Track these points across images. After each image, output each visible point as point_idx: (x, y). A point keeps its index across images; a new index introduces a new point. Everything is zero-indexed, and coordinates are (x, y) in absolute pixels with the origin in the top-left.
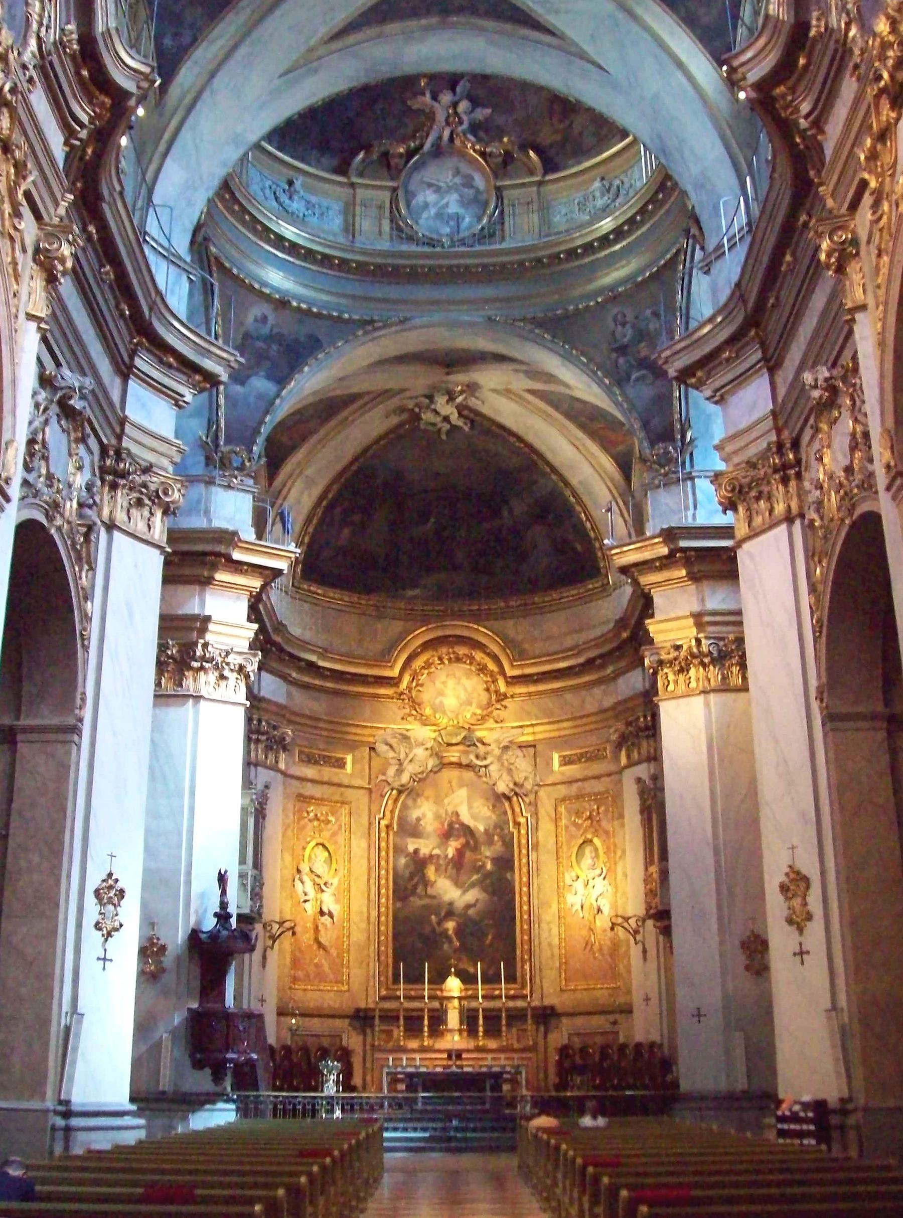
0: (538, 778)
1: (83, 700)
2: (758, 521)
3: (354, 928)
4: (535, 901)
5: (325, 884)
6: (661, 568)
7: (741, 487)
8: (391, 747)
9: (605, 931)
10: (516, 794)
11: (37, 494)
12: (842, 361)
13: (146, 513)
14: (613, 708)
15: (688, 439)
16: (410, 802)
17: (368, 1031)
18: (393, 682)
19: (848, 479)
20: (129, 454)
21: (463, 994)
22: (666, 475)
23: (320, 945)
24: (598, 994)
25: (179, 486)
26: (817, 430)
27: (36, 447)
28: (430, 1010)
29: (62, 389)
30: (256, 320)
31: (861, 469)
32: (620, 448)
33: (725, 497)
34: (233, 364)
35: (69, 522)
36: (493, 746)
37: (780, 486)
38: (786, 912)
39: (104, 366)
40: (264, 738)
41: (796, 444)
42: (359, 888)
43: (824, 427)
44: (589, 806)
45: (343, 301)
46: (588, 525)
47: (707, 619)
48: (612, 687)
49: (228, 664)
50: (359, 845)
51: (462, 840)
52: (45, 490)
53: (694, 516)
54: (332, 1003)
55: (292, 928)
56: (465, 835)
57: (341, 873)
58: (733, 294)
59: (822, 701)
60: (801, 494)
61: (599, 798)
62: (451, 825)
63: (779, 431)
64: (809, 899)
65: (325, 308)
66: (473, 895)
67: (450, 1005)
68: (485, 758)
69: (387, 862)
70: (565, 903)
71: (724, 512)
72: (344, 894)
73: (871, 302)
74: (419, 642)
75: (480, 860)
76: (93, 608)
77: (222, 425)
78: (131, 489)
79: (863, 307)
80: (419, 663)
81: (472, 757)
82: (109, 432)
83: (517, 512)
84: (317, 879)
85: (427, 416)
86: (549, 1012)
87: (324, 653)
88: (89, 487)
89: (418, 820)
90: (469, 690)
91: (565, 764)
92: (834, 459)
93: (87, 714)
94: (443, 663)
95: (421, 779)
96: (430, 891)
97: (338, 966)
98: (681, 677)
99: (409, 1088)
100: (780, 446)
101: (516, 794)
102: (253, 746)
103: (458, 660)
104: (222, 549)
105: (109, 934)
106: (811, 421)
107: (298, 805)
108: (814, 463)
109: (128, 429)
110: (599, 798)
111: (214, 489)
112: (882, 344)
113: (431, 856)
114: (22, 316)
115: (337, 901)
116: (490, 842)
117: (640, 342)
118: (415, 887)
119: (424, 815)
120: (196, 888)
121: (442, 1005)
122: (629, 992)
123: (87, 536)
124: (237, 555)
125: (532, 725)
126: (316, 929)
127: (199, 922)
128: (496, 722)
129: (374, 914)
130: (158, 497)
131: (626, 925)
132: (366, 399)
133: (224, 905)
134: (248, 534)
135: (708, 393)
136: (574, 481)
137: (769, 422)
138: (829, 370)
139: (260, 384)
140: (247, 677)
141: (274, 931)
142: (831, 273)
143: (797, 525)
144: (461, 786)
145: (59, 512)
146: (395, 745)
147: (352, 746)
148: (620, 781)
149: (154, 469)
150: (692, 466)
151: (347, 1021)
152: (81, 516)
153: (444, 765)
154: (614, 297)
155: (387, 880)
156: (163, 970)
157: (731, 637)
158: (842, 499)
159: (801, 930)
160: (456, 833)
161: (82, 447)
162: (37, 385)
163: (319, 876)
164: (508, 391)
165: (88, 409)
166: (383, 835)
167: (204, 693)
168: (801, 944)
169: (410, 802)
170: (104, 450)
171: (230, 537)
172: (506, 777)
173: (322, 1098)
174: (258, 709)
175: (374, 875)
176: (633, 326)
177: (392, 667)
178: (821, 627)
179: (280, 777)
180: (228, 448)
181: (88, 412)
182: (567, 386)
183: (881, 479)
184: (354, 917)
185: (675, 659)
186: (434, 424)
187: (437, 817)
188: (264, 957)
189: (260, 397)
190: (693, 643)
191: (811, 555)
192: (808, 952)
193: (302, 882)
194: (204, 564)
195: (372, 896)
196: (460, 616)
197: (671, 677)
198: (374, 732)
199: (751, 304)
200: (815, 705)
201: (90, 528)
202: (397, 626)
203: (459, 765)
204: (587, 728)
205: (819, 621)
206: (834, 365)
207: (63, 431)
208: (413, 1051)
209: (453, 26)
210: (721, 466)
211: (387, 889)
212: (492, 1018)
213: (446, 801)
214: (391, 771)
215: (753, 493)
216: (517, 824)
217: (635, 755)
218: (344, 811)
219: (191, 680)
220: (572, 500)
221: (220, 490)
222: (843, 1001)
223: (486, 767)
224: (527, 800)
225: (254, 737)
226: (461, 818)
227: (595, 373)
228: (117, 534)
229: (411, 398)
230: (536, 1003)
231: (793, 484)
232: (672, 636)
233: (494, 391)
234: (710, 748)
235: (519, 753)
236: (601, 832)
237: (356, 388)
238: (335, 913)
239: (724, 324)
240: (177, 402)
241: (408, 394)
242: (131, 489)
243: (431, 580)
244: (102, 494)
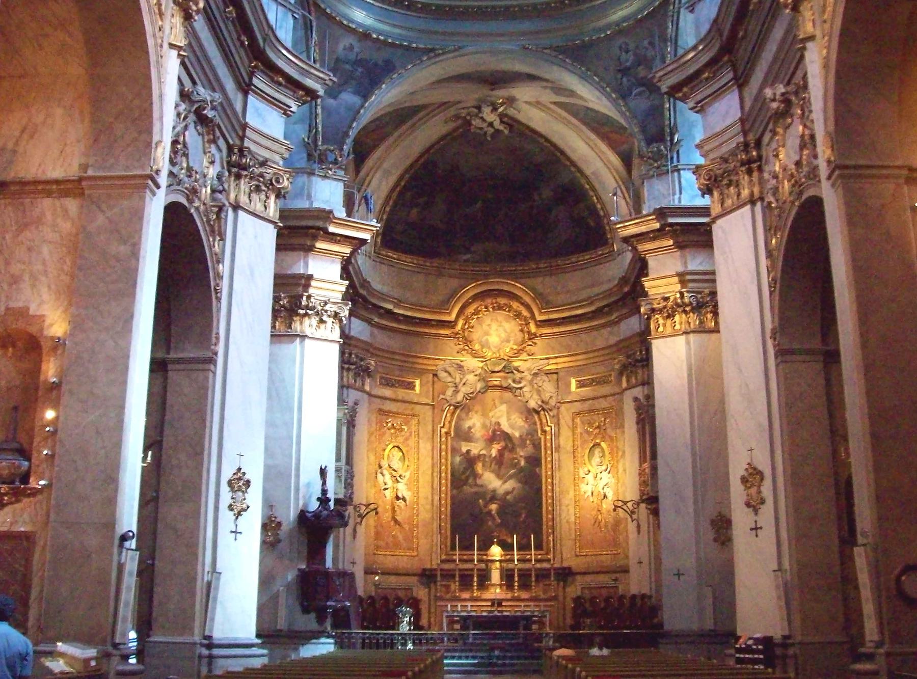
0: (560, 397)
1: (218, 338)
2: (729, 202)
3: (421, 509)
4: (557, 489)
5: (400, 476)
6: (654, 239)
7: (716, 176)
8: (450, 374)
9: (609, 511)
10: (544, 409)
11: (180, 182)
12: (795, 81)
13: (263, 197)
14: (616, 345)
15: (676, 140)
16: (463, 415)
17: (432, 585)
18: (450, 325)
19: (797, 171)
20: (250, 152)
21: (503, 558)
22: (658, 168)
23: (396, 521)
24: (603, 558)
25: (288, 176)
26: (775, 133)
27: (179, 146)
28: (478, 570)
29: (198, 101)
30: (344, 49)
31: (809, 163)
32: (625, 147)
33: (703, 185)
34: (327, 82)
35: (204, 204)
36: (526, 373)
37: (746, 177)
38: (745, 498)
39: (230, 85)
40: (353, 367)
41: (758, 144)
42: (425, 480)
43: (780, 130)
44: (599, 419)
45: (410, 34)
46: (599, 206)
47: (689, 277)
48: (616, 328)
49: (326, 311)
50: (425, 447)
51: (503, 444)
52: (186, 179)
53: (680, 199)
54: (405, 566)
55: (376, 509)
56: (504, 440)
57: (412, 468)
58: (712, 26)
59: (775, 339)
60: (761, 182)
61: (606, 412)
62: (494, 431)
63: (745, 133)
64: (762, 488)
65: (398, 39)
66: (510, 485)
67: (493, 567)
68: (520, 382)
69: (446, 460)
70: (579, 491)
71: (703, 197)
72: (414, 483)
73: (818, 33)
74: (471, 294)
75: (516, 459)
76: (224, 269)
77: (320, 129)
78: (251, 178)
79: (812, 38)
80: (471, 310)
81: (510, 381)
82: (234, 135)
83: (544, 196)
84: (393, 472)
85: (476, 122)
86: (567, 571)
87: (399, 303)
88: (219, 177)
89: (470, 428)
90: (508, 330)
91: (581, 387)
92: (787, 155)
93: (221, 349)
94: (488, 311)
95: (472, 397)
96: (479, 482)
97: (409, 538)
98: (669, 322)
99: (463, 628)
100: (746, 145)
101: (544, 409)
102: (345, 374)
103: (500, 308)
104: (320, 224)
105: (239, 514)
106: (770, 126)
107: (379, 417)
108: (772, 158)
109: (248, 132)
110: (606, 412)
111: (315, 179)
112: (826, 66)
113: (479, 456)
114: (166, 46)
115: (409, 489)
116: (523, 445)
117: (639, 65)
118: (467, 478)
119: (474, 425)
120: (303, 480)
121: (487, 566)
122: (627, 557)
123: (218, 214)
124: (332, 229)
125: (556, 358)
126: (393, 508)
127: (306, 505)
128: (529, 355)
129: (437, 498)
130: (272, 184)
131: (625, 507)
132: (430, 109)
133: (324, 492)
134: (340, 212)
135: (692, 104)
136: (588, 172)
137: (738, 127)
138: (785, 86)
139: (349, 98)
140: (341, 321)
141: (361, 511)
142: (788, 11)
143: (759, 204)
144: (502, 403)
145: (197, 196)
146: (452, 372)
147: (421, 373)
148: (621, 401)
149: (269, 163)
150: (678, 161)
151: (415, 579)
152: (214, 199)
153: (489, 387)
154: (620, 31)
155: (446, 473)
156: (279, 541)
157: (707, 291)
158: (793, 186)
159: (756, 512)
160: (498, 438)
161: (213, 146)
162: (178, 99)
163: (394, 470)
164: (538, 103)
165: (217, 117)
166: (443, 439)
167: (308, 332)
168: (756, 522)
169: (463, 415)
170: (230, 148)
171: (327, 215)
172: (536, 396)
173: (398, 634)
174: (350, 345)
175: (437, 469)
176: (635, 55)
177: (449, 314)
178: (775, 283)
179: (366, 396)
180: (325, 147)
181: (218, 120)
182: (581, 98)
183: (824, 171)
184: (422, 501)
185: (665, 307)
186: (481, 129)
187: (484, 426)
188: (355, 531)
189: (349, 108)
190: (678, 295)
191: (769, 230)
192: (761, 528)
193: (383, 475)
194: (306, 235)
195: (435, 486)
196: (501, 274)
197: (661, 321)
198: (437, 362)
199: (726, 33)
200: (770, 343)
201: (221, 209)
202: (454, 283)
203: (501, 388)
204: (597, 360)
205: (774, 280)
206: (788, 83)
207: (199, 134)
208: (465, 600)
210: (701, 161)
211: (446, 480)
212: (525, 575)
213: (491, 414)
214: (449, 392)
215: (725, 182)
216: (544, 432)
217: (633, 381)
218: (414, 421)
219: (298, 323)
220: (587, 187)
221: (319, 179)
222: (786, 565)
223: (521, 388)
224: (551, 414)
225: (346, 366)
226: (502, 427)
227: (604, 89)
228: (241, 213)
229: (463, 108)
230: (557, 565)
231: (755, 174)
232: (661, 290)
233: (526, 102)
234: (690, 376)
235: (545, 378)
236: (607, 437)
237: (421, 100)
238: (407, 498)
239: (705, 51)
240: (286, 111)
242: (251, 178)
243: (477, 247)
244: (229, 182)
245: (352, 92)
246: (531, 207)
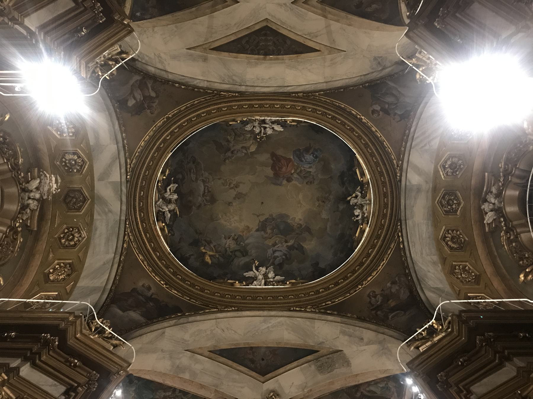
30: (143, 286)
117: (388, 300)
209: (271, 59)
245: (139, 314)
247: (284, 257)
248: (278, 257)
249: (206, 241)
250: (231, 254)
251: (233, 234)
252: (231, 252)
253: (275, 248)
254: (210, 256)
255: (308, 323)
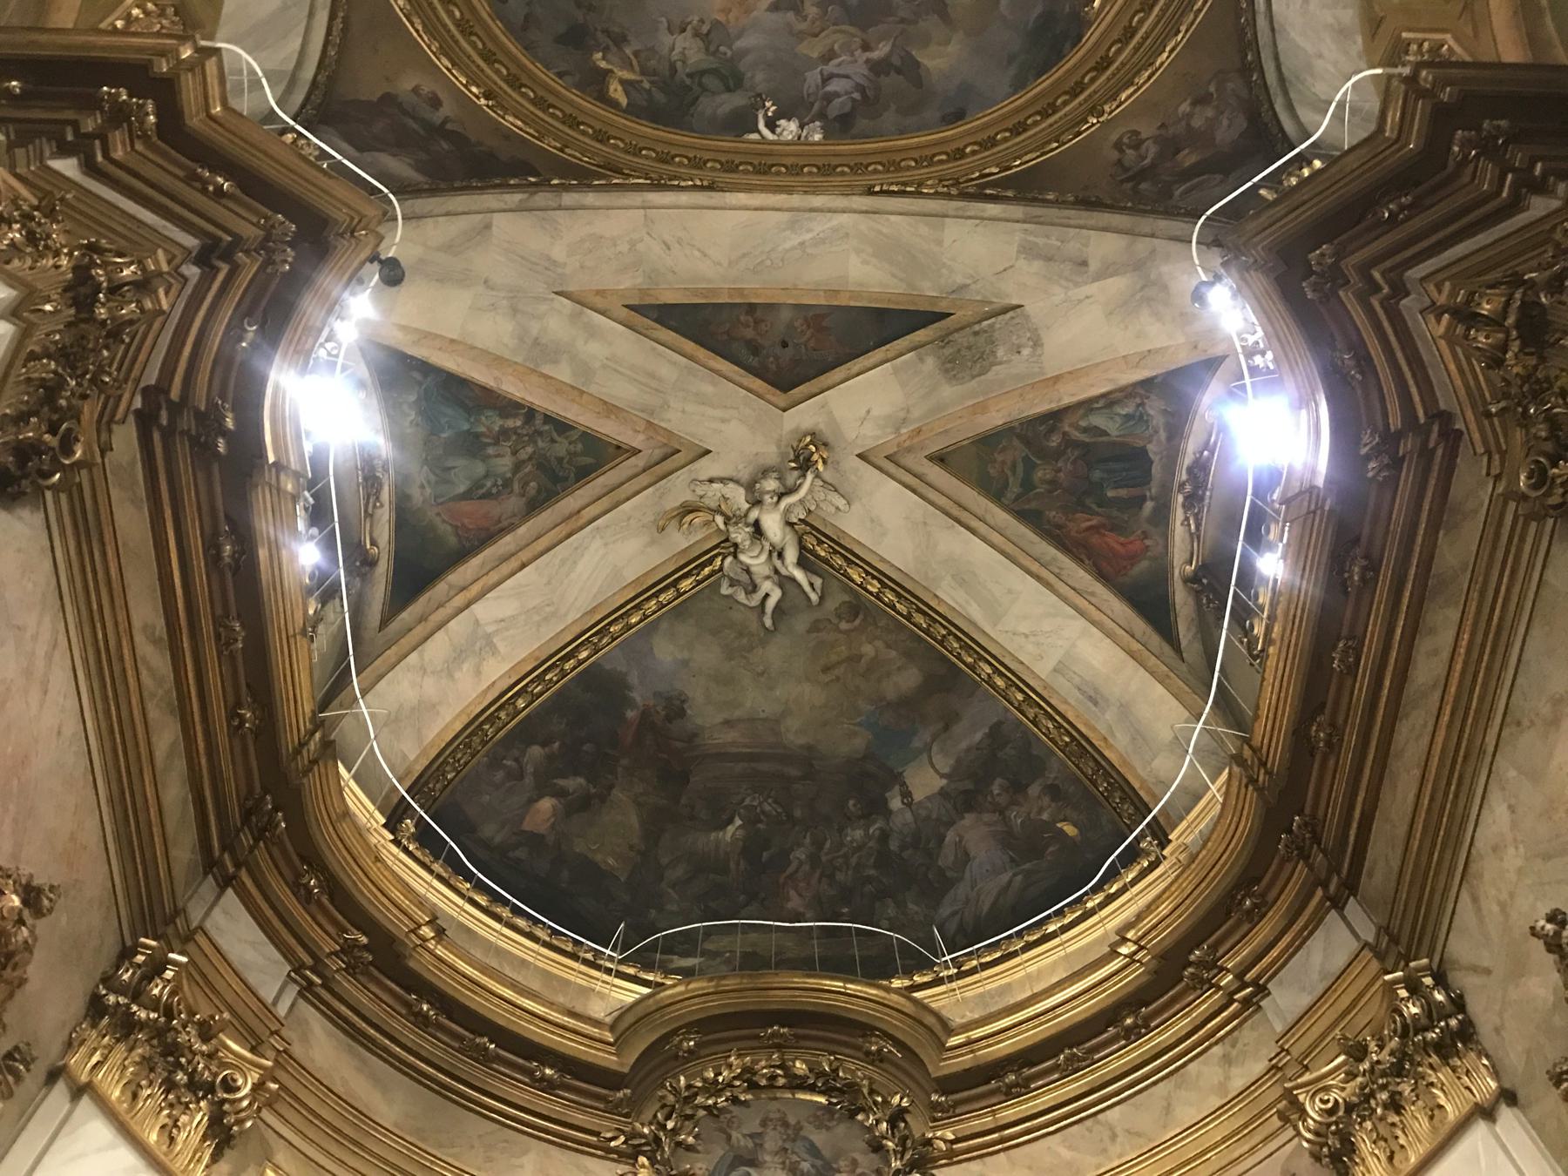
30: (416, 90)
83: (918, 795)
90: (826, 1153)
117: (1178, 151)
241: (706, 468)
245: (409, 164)
246: (885, 836)
247: (856, 95)
248: (836, 95)
249: (606, 32)
250: (688, 81)
251: (696, 19)
252: (690, 75)
253: (831, 67)
254: (623, 82)
255: (923, 228)
